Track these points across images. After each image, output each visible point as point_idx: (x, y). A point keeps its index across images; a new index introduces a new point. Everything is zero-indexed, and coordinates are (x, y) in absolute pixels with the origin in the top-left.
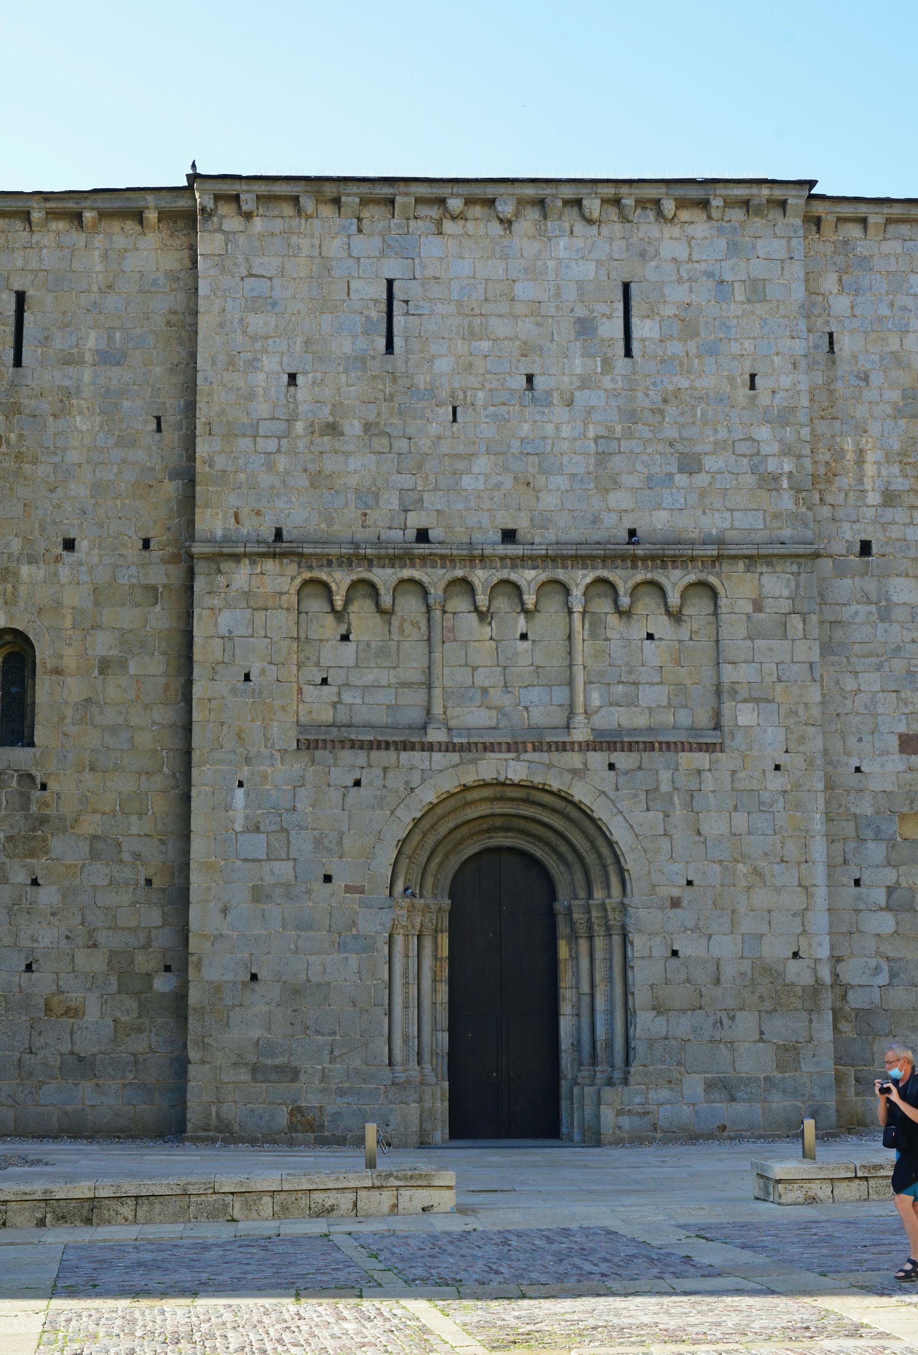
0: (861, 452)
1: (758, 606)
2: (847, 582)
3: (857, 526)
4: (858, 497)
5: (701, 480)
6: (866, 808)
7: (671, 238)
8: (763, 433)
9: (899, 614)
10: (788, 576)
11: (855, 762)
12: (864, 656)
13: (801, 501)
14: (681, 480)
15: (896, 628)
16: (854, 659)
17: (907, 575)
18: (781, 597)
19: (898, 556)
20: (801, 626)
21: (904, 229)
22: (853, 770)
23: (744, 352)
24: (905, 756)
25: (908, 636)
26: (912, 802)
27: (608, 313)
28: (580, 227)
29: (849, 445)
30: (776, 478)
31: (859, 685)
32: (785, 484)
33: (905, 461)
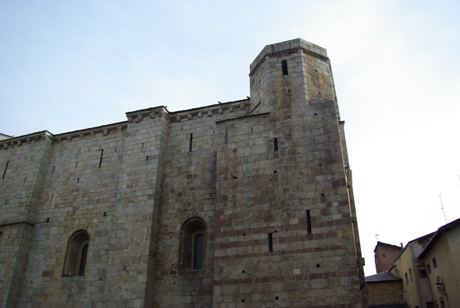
0: (53, 195)
1: (9, 237)
2: (42, 229)
3: (48, 214)
4: (49, 207)
5: (8, 206)
6: (30, 293)
7: (20, 150)
8: (23, 192)
9: (51, 237)
10: (17, 228)
11: (31, 280)
12: (41, 249)
13: (26, 208)
14: (4, 206)
15: (50, 240)
16: (38, 250)
17: (55, 226)
18: (15, 234)
19: (54, 221)
20: (17, 241)
21: (76, 139)
22: (31, 282)
23: (26, 173)
24: (43, 277)
25: (52, 243)
26: (42, 291)
27: (2, 169)
28: (4, 151)
29: (51, 194)
30: (22, 203)
31: (37, 257)
32: (24, 204)
33: (62, 196)
